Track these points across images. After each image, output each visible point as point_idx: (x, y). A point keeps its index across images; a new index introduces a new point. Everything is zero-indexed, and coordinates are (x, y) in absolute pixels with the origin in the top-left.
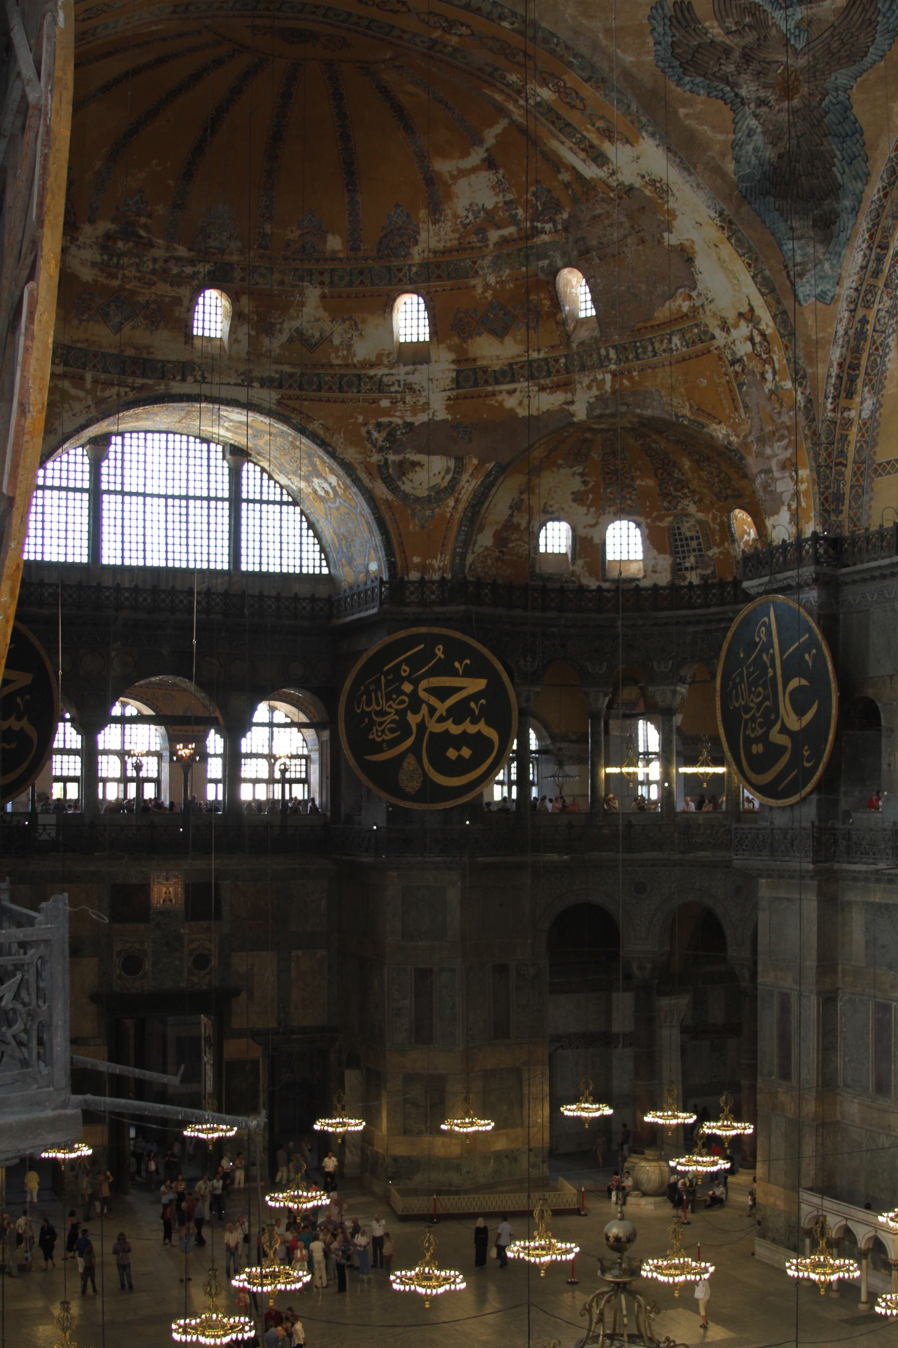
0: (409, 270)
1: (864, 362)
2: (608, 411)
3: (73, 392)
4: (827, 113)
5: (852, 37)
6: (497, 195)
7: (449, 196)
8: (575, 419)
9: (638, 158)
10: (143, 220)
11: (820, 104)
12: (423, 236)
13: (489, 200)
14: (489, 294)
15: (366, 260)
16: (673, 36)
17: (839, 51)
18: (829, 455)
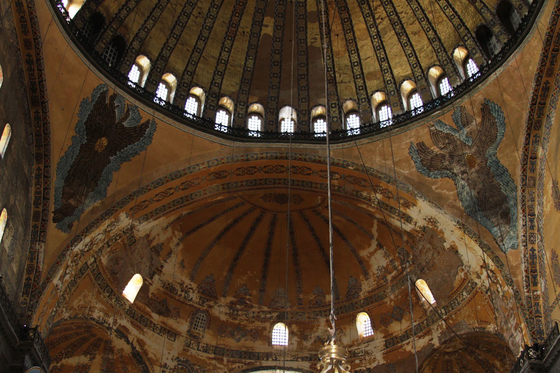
0: (360, 302)
1: (538, 268)
2: (447, 338)
3: (219, 365)
4: (490, 167)
5: (489, 133)
6: (386, 259)
7: (369, 266)
8: (435, 347)
9: (420, 211)
10: (248, 297)
11: (486, 165)
12: (363, 286)
13: (384, 262)
14: (392, 303)
15: (343, 302)
16: (421, 157)
17: (486, 140)
18: (531, 313)
